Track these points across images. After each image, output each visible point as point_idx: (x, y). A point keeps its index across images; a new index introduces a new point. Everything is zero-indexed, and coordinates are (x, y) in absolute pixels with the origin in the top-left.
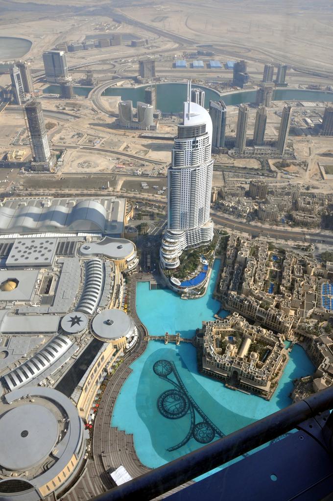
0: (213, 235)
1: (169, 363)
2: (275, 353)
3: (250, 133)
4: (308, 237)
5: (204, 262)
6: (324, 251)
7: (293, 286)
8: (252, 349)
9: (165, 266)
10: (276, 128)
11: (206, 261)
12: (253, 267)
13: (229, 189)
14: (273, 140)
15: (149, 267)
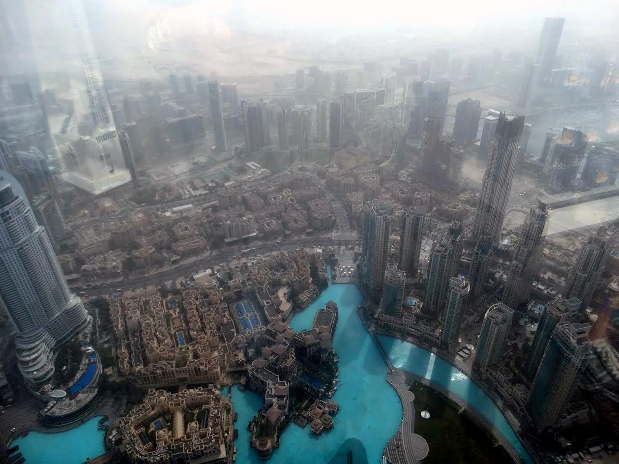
5: (88, 350)
9: (34, 382)
13: (87, 250)
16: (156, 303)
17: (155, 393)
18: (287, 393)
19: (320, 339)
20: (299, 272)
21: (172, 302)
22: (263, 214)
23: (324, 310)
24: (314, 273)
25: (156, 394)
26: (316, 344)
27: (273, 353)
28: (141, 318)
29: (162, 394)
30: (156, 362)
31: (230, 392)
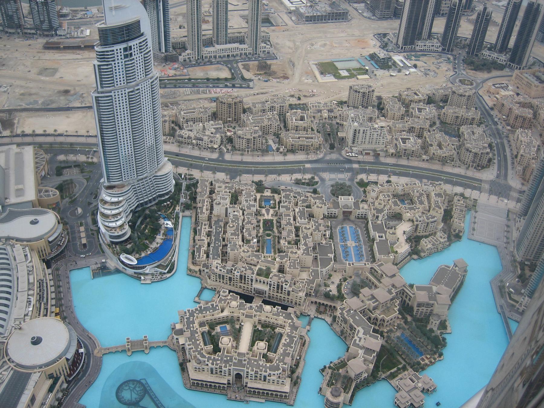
0: (174, 182)
1: (139, 382)
2: (288, 336)
3: (207, 29)
4: (308, 166)
5: (167, 224)
6: (333, 183)
7: (297, 238)
8: (257, 336)
9: (109, 239)
10: (243, 17)
11: (169, 223)
12: (238, 221)
14: (242, 34)
15: (85, 245)
16: (249, 195)
17: (228, 296)
18: (378, 349)
19: (436, 300)
20: (429, 211)
21: (267, 200)
22: (400, 126)
23: (449, 267)
24: (448, 215)
25: (229, 297)
26: (428, 305)
27: (373, 297)
28: (230, 207)
29: (235, 300)
30: (236, 261)
31: (309, 324)
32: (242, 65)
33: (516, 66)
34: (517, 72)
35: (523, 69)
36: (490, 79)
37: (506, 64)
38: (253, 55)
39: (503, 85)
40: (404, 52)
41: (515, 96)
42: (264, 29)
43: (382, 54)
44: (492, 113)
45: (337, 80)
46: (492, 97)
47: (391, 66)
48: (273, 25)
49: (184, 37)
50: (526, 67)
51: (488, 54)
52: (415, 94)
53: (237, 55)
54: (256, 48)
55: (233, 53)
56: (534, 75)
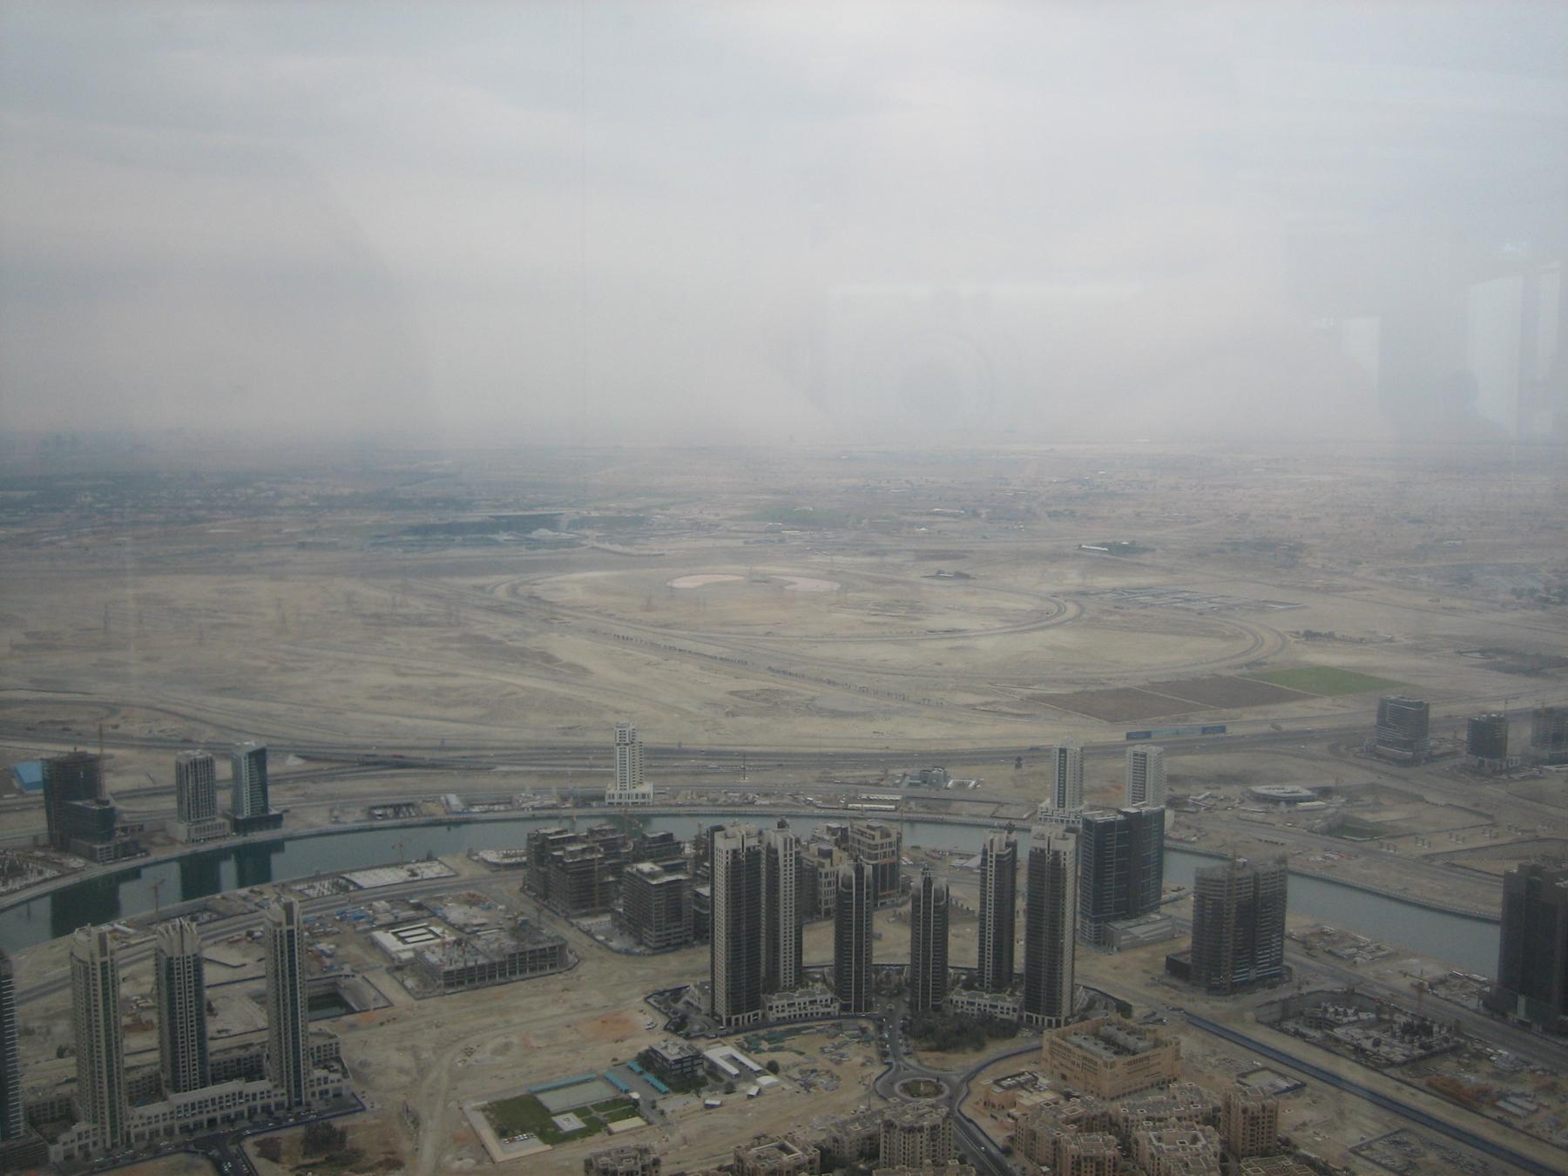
10: (258, 998)
14: (253, 1050)
32: (257, 1144)
33: (1047, 1018)
34: (1049, 1035)
35: (1067, 1023)
36: (984, 1067)
37: (1021, 1017)
38: (289, 1109)
39: (1022, 1079)
40: (737, 1032)
41: (1062, 1102)
42: (317, 1028)
43: (673, 1049)
44: (1009, 1163)
45: (548, 1147)
46: (1000, 1118)
47: (704, 1078)
48: (351, 1011)
49: (68, 1081)
50: (1073, 1016)
51: (965, 999)
52: (783, 1148)
53: (240, 1115)
54: (298, 1086)
55: (223, 1112)
56: (1096, 1035)
